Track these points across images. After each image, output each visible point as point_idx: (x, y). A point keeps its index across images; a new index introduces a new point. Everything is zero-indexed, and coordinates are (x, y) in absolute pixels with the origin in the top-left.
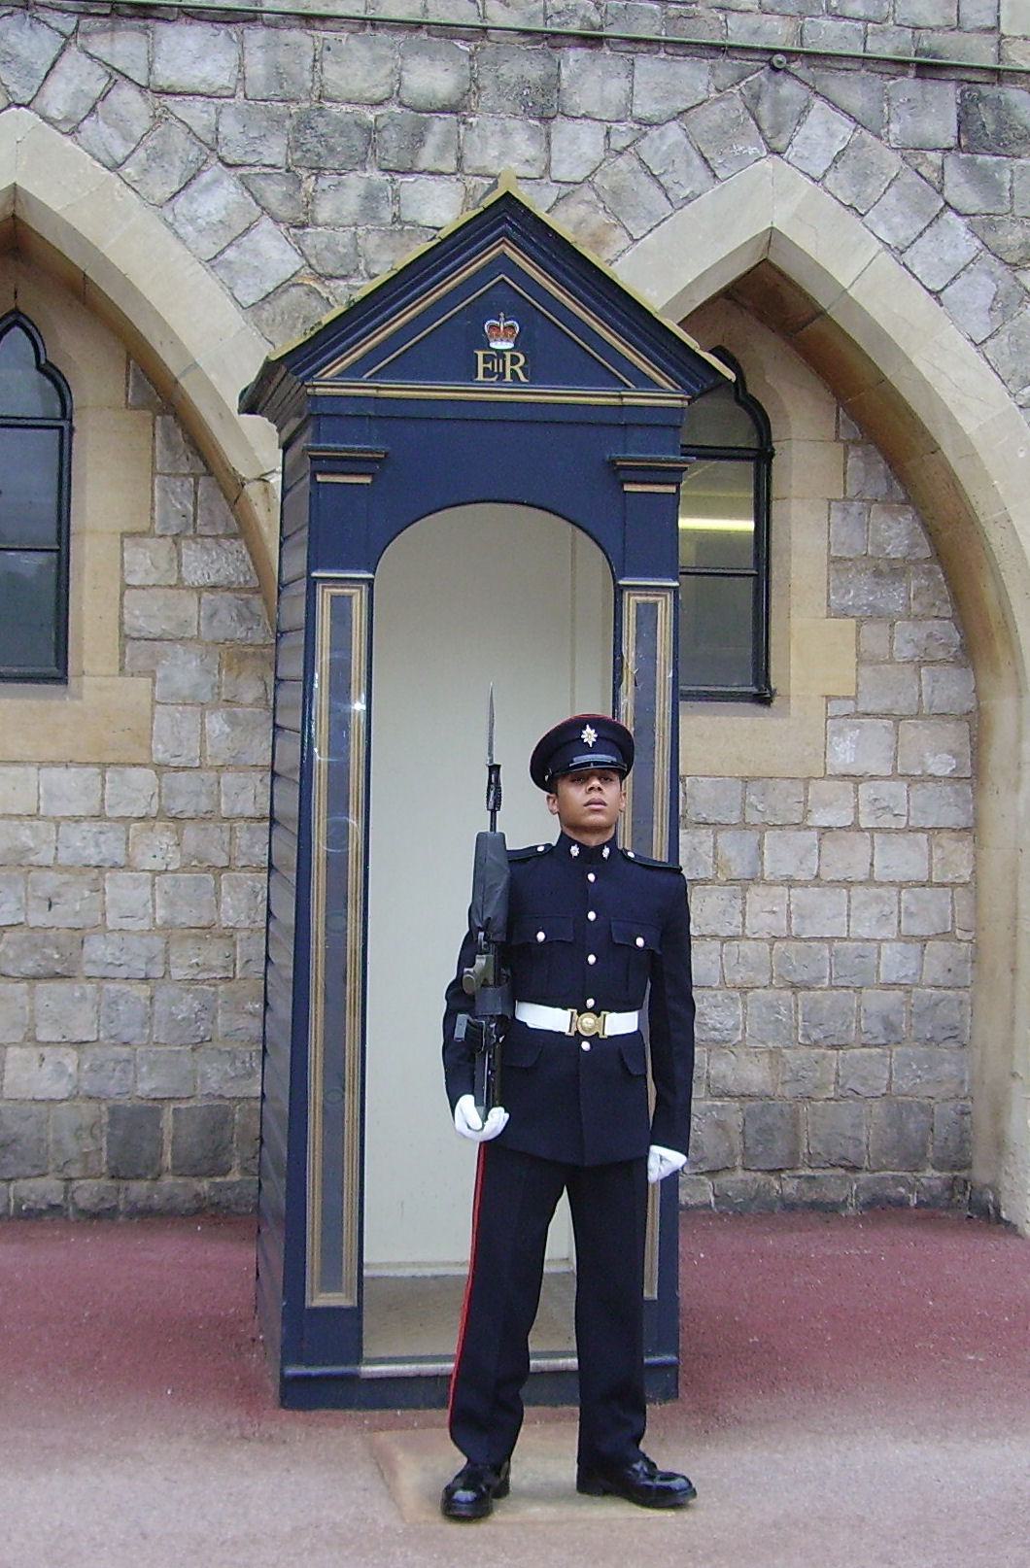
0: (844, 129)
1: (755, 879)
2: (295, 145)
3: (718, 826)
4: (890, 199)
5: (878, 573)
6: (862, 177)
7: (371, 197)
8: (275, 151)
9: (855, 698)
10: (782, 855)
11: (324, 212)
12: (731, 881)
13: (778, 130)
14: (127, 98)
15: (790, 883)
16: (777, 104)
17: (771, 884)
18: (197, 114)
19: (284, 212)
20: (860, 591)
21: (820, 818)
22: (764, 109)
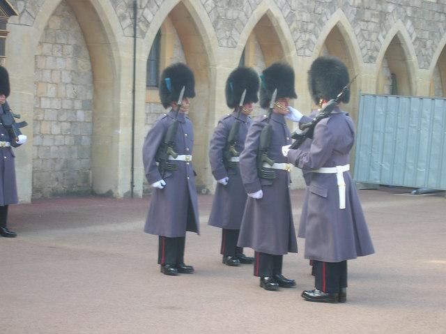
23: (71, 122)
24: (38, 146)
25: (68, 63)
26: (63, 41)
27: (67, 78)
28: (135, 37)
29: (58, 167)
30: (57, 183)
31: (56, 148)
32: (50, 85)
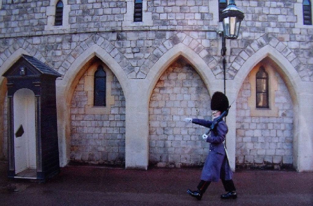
0: (103, 40)
1: (103, 126)
2: (45, 48)
3: (98, 121)
4: (108, 47)
5: (117, 90)
6: (105, 45)
7: (53, 53)
8: (43, 49)
9: (114, 105)
10: (106, 124)
11: (48, 55)
12: (99, 127)
13: (96, 40)
14: (31, 46)
15: (106, 127)
16: (96, 38)
17: (104, 127)
18: (36, 47)
19: (44, 55)
20: (115, 92)
21: (110, 119)
22: (94, 39)
23: (196, 128)
24: (172, 141)
25: (194, 97)
26: (188, 85)
27: (191, 104)
28: (225, 79)
29: (186, 152)
30: (186, 160)
31: (185, 142)
32: (179, 109)
